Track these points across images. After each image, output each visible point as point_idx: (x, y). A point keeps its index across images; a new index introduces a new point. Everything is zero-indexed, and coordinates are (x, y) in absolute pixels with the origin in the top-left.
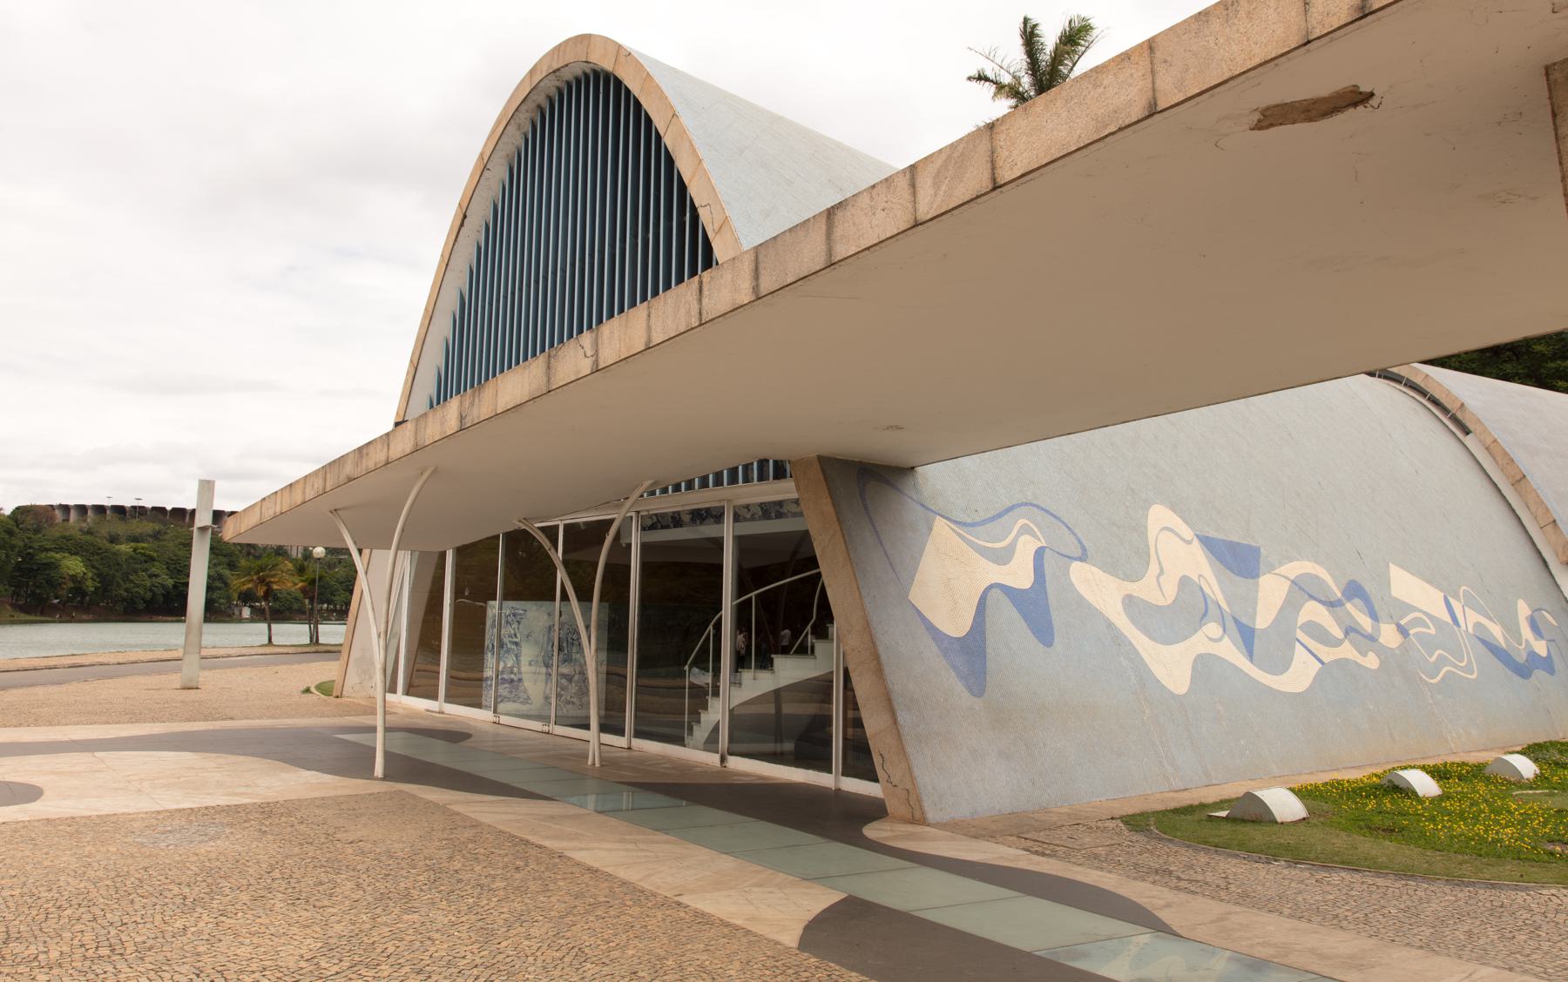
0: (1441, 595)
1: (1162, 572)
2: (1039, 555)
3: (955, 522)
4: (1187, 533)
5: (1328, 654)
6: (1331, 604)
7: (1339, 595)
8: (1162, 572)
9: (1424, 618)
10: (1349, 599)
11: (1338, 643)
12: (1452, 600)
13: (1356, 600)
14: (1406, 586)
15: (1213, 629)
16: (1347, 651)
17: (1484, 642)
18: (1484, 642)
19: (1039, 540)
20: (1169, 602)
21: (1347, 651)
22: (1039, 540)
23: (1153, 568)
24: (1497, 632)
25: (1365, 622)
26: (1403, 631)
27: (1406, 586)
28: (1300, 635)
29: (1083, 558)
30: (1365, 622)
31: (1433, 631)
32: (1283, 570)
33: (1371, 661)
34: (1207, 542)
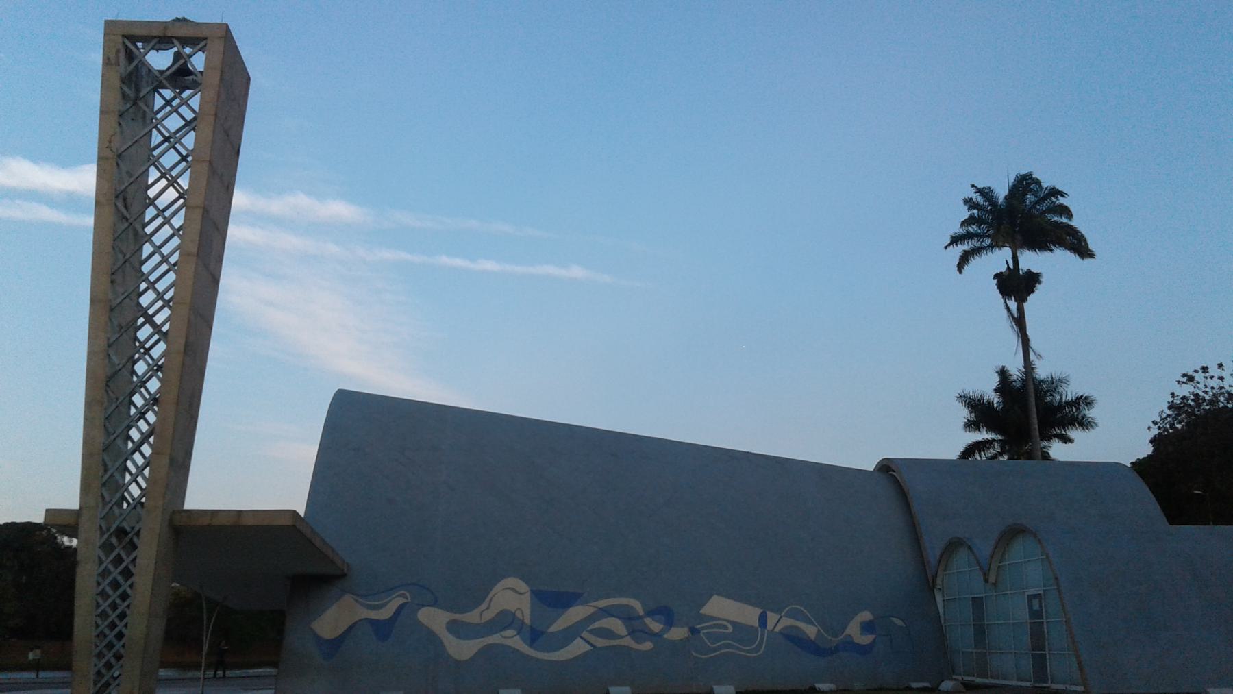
0: (759, 611)
3: (358, 596)
4: (523, 587)
5: (600, 642)
6: (628, 617)
7: (641, 613)
8: (488, 608)
9: (725, 623)
10: (650, 614)
11: (621, 637)
12: (769, 614)
13: (658, 617)
16: (628, 642)
19: (407, 599)
20: (483, 621)
21: (628, 642)
22: (407, 599)
23: (484, 606)
24: (811, 631)
25: (656, 626)
26: (694, 631)
28: (585, 634)
29: (435, 604)
30: (656, 626)
31: (731, 629)
32: (595, 604)
33: (647, 646)
34: (533, 592)
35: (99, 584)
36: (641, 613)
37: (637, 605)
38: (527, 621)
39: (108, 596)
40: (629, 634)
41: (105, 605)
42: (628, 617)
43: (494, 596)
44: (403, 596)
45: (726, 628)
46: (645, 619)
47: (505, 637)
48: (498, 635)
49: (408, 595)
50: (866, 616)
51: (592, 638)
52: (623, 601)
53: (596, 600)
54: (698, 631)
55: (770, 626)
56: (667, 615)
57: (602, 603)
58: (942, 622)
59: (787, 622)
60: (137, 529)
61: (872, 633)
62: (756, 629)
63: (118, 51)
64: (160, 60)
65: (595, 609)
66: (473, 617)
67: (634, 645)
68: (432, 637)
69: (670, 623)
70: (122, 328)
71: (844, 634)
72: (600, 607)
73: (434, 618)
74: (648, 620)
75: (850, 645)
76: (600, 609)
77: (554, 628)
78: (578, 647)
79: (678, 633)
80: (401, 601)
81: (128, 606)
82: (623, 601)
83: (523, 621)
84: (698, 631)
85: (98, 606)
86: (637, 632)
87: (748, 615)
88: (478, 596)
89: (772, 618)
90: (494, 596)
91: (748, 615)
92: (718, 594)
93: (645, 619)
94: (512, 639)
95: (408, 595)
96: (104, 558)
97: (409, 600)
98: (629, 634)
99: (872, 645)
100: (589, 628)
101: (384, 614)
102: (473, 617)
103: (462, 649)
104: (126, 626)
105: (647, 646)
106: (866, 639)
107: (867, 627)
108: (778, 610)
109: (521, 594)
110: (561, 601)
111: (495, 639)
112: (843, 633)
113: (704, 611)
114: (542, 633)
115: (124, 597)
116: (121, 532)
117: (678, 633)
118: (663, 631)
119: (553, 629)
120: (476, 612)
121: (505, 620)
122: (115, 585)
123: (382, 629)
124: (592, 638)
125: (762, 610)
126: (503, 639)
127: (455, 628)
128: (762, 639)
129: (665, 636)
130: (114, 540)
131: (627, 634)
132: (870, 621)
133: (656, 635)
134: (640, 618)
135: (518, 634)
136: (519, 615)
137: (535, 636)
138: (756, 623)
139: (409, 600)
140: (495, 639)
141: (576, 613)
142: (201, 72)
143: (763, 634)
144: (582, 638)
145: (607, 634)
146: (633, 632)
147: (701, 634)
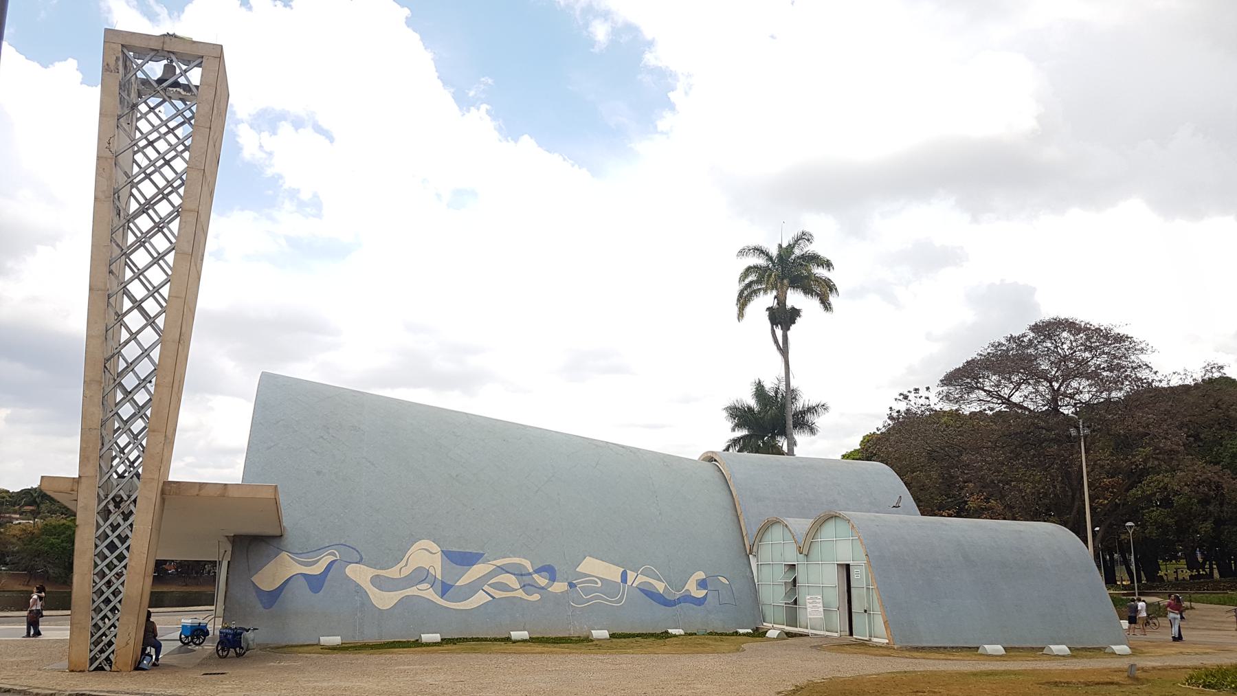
1: (406, 565)
2: (332, 563)
4: (436, 548)
5: (498, 594)
6: (521, 574)
7: (531, 571)
8: (406, 565)
10: (536, 571)
14: (593, 567)
15: (424, 586)
16: (520, 594)
17: (642, 590)
18: (642, 590)
21: (520, 594)
23: (403, 563)
24: (660, 587)
25: (542, 581)
26: (571, 585)
27: (593, 567)
31: (600, 584)
32: (494, 562)
33: (536, 597)
34: (442, 551)
35: (96, 546)
36: (531, 571)
37: (527, 564)
38: (439, 577)
39: (106, 557)
40: (521, 588)
41: (102, 565)
42: (521, 574)
44: (334, 555)
45: (597, 584)
46: (534, 576)
49: (337, 553)
50: (701, 575)
51: (491, 591)
52: (516, 560)
53: (495, 559)
55: (629, 583)
56: (550, 572)
57: (499, 562)
58: (756, 581)
59: (642, 579)
60: (133, 498)
61: (705, 589)
63: (117, 59)
64: (155, 70)
65: (495, 567)
66: (393, 573)
68: (359, 589)
69: (553, 579)
70: (119, 316)
71: (685, 589)
72: (498, 565)
73: (360, 574)
74: (535, 576)
75: (688, 598)
76: (498, 567)
78: (480, 598)
79: (559, 587)
80: (332, 558)
81: (125, 567)
82: (516, 560)
85: (96, 565)
86: (527, 587)
87: (613, 573)
88: (398, 556)
89: (631, 575)
91: (614, 573)
92: (590, 556)
93: (534, 576)
94: (426, 592)
95: (337, 553)
96: (101, 522)
97: (338, 558)
98: (521, 588)
99: (705, 597)
100: (489, 583)
102: (393, 573)
103: (384, 600)
104: (122, 584)
105: (536, 597)
106: (700, 594)
107: (702, 584)
108: (636, 570)
109: (431, 553)
110: (466, 560)
112: (683, 588)
114: (451, 586)
115: (121, 558)
116: (118, 501)
117: (559, 587)
121: (421, 576)
122: (112, 547)
123: (315, 583)
124: (491, 591)
126: (419, 591)
127: (377, 582)
130: (111, 507)
132: (704, 579)
133: (543, 588)
134: (530, 574)
135: (432, 587)
137: (445, 589)
139: (338, 558)
141: (478, 570)
142: (197, 87)
144: (483, 590)
145: (503, 587)
146: (524, 586)
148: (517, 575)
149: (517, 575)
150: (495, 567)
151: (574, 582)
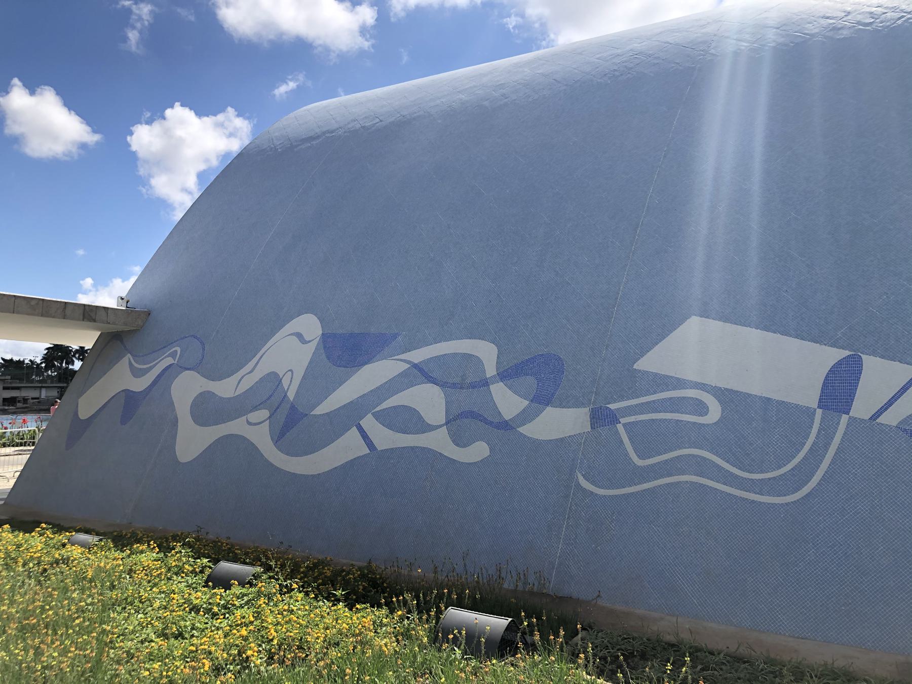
7: (491, 371)
10: (504, 375)
15: (264, 414)
28: (368, 423)
31: (715, 412)
33: (478, 451)
38: (291, 395)
40: (447, 423)
43: (264, 354)
44: (173, 355)
45: (701, 408)
47: (249, 423)
48: (244, 418)
54: (612, 418)
57: (418, 356)
62: (810, 413)
65: (408, 366)
67: (451, 451)
72: (416, 362)
76: (415, 366)
77: (320, 410)
80: (169, 361)
83: (286, 395)
84: (612, 418)
90: (264, 354)
101: (139, 385)
105: (478, 451)
111: (236, 427)
113: (643, 364)
118: (526, 417)
119: (320, 410)
120: (233, 380)
125: (847, 353)
128: (817, 453)
129: (527, 430)
131: (444, 422)
133: (506, 426)
134: (486, 383)
136: (285, 383)
138: (810, 397)
140: (236, 427)
143: (826, 435)
147: (620, 427)
148: (454, 386)
149: (454, 386)
150: (408, 366)
151: (612, 406)
